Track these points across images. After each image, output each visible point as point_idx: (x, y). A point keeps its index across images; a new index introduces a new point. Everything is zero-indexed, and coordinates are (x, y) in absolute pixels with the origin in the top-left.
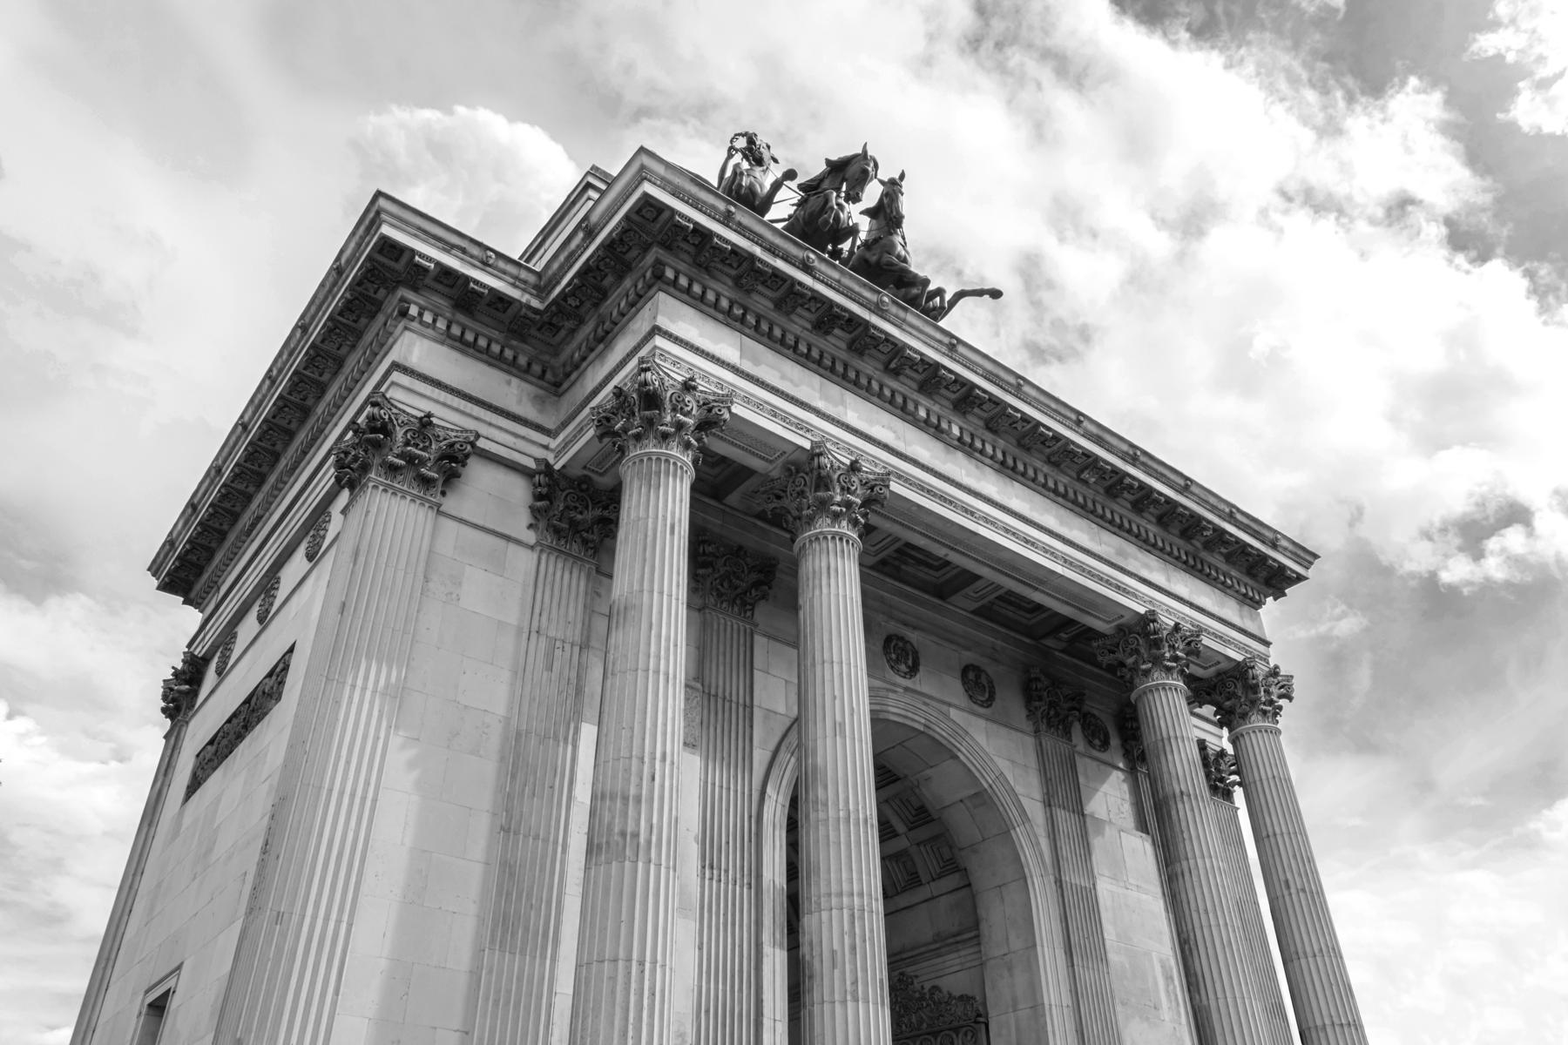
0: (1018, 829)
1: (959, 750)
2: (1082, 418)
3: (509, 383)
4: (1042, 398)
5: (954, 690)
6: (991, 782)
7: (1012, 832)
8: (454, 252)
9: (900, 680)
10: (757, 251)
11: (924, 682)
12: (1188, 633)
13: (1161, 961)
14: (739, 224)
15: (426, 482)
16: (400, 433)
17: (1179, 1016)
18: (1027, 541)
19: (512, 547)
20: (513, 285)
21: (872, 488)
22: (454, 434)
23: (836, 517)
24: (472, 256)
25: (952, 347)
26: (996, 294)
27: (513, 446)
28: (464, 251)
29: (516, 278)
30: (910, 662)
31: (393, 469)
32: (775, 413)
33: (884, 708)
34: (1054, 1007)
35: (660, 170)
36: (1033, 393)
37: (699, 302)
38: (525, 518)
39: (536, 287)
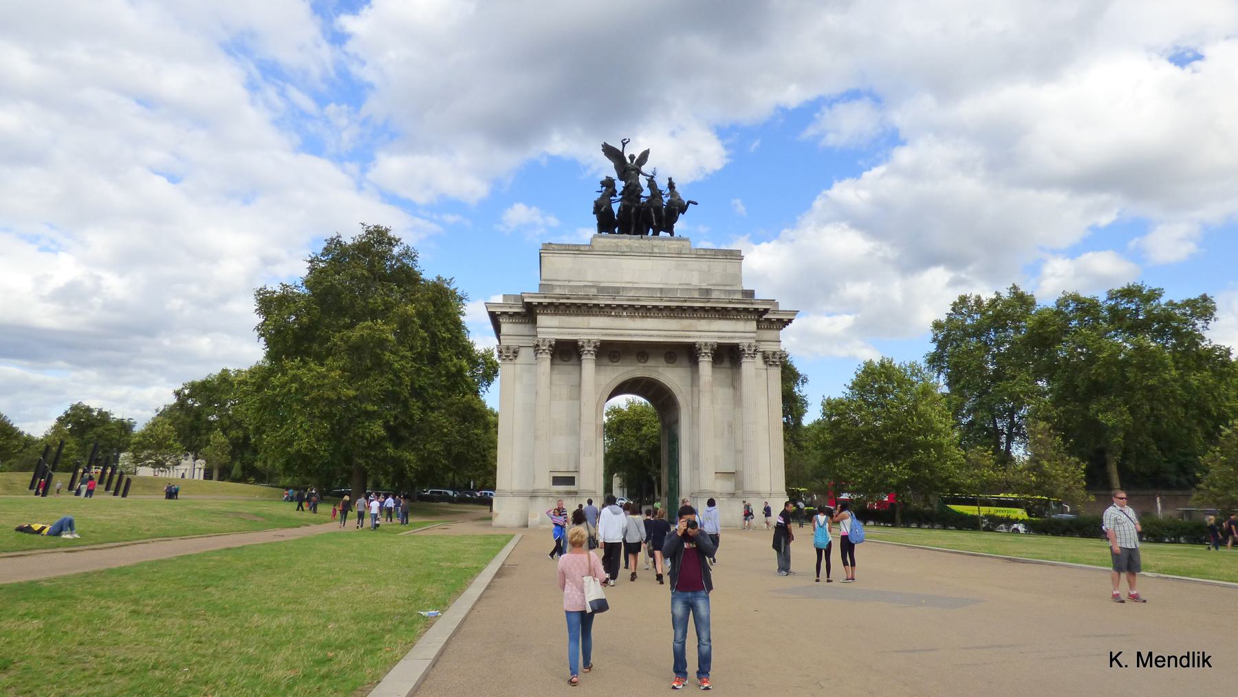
5: (662, 361)
9: (642, 365)
10: (554, 301)
11: (650, 363)
25: (614, 298)
32: (569, 334)
35: (527, 295)
37: (545, 314)
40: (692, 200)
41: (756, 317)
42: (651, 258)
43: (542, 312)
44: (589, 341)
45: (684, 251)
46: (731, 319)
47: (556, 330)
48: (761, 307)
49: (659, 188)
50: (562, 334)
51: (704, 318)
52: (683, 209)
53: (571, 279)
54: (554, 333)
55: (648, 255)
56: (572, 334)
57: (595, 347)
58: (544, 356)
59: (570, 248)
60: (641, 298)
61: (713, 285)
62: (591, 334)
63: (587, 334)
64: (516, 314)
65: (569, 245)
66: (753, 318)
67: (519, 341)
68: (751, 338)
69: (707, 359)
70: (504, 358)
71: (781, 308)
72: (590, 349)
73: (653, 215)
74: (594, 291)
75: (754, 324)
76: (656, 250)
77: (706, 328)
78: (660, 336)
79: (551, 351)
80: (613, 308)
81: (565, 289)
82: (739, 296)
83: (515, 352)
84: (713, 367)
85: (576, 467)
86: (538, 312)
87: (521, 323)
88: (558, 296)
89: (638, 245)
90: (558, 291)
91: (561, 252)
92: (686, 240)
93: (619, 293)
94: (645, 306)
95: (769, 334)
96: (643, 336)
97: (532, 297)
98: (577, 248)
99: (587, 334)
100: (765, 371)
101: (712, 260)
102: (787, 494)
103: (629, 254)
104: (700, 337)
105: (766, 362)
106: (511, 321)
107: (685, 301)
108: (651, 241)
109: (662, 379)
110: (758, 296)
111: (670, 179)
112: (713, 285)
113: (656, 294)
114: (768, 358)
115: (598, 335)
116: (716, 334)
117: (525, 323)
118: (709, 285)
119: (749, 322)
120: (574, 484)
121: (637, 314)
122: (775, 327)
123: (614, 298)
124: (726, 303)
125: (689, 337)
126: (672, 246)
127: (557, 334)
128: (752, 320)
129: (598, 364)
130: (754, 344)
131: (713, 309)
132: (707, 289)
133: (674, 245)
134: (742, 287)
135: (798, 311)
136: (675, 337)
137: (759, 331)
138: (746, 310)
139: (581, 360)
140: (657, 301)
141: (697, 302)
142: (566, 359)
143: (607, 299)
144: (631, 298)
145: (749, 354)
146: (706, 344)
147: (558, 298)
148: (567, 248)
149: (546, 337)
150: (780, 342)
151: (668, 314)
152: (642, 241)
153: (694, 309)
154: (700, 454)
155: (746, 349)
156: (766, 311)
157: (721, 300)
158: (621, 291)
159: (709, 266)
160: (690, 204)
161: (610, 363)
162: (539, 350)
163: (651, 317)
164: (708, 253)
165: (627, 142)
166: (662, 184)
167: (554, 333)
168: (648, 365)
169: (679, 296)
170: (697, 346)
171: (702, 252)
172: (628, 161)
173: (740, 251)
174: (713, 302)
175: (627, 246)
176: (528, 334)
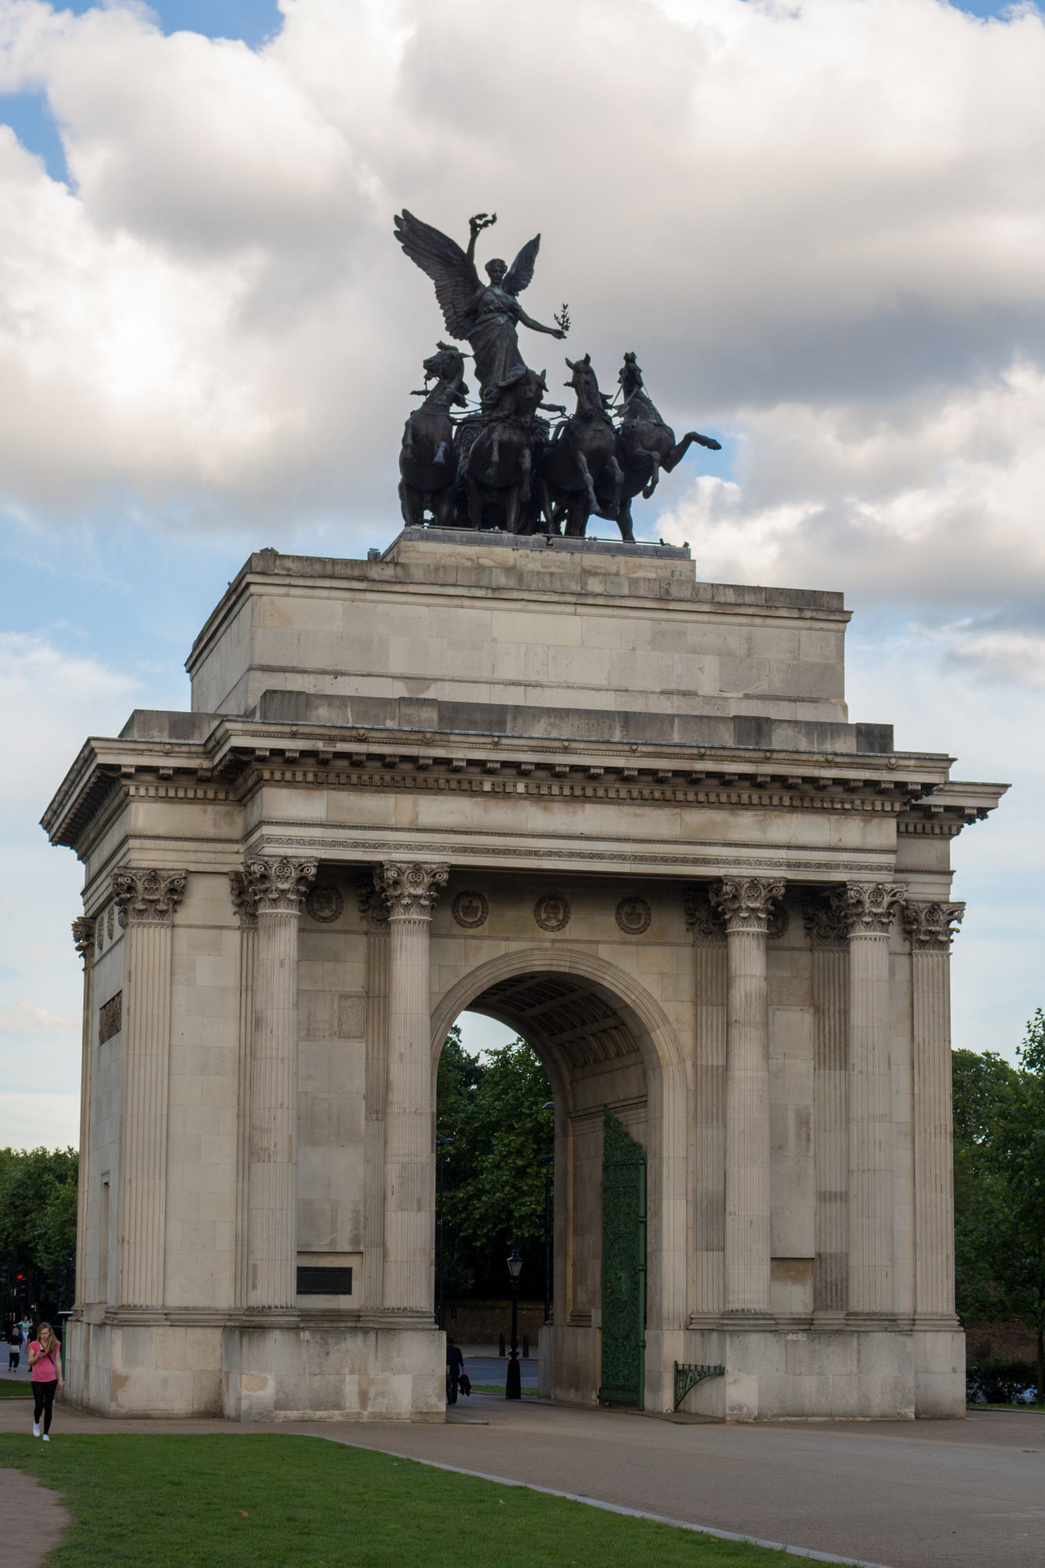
0: (658, 1031)
1: (604, 979)
2: (634, 747)
3: (205, 811)
4: (591, 746)
6: (634, 997)
7: (653, 1035)
8: (145, 753)
9: (551, 935)
10: (320, 745)
12: (772, 881)
13: (798, 1113)
14: (303, 734)
15: (162, 913)
16: (140, 886)
17: (807, 1149)
18: (592, 856)
19: (225, 932)
20: (189, 757)
21: (434, 876)
22: (172, 873)
23: (407, 906)
24: (157, 751)
26: (714, 445)
27: (214, 861)
28: (151, 751)
29: (190, 753)
30: (561, 917)
31: (141, 912)
32: (356, 845)
33: (529, 963)
34: (671, 1161)
36: (582, 745)
37: (292, 784)
38: (232, 909)
39: (204, 753)
40: (701, 432)
41: (897, 807)
42: (580, 609)
43: (278, 776)
44: (417, 867)
45: (675, 592)
46: (822, 811)
47: (317, 833)
48: (915, 778)
49: (603, 389)
50: (334, 844)
51: (749, 806)
52: (672, 455)
53: (341, 667)
54: (312, 842)
55: (573, 599)
56: (364, 846)
57: (434, 886)
58: (282, 910)
59: (339, 570)
60: (574, 745)
61: (763, 698)
62: (421, 847)
63: (408, 847)
64: (178, 771)
65: (334, 562)
66: (888, 808)
67: (192, 857)
68: (880, 868)
69: (755, 929)
70: (142, 907)
71: (955, 774)
72: (419, 891)
73: (588, 475)
74: (429, 717)
75: (892, 824)
76: (595, 585)
77: (755, 835)
78: (622, 857)
79: (303, 894)
80: (491, 772)
81: (346, 706)
82: (847, 745)
83: (172, 891)
84: (769, 949)
85: (356, 1240)
86: (267, 775)
87: (194, 801)
88: (335, 732)
89: (539, 568)
90: (323, 714)
91: (309, 582)
92: (683, 553)
93: (501, 724)
94: (584, 769)
95: (922, 851)
96: (572, 855)
97: (254, 734)
98: (356, 572)
99: (408, 847)
100: (905, 960)
101: (758, 621)
102: (962, 1323)
103: (515, 595)
104: (737, 862)
105: (908, 934)
106: (162, 792)
107: (701, 757)
108: (577, 556)
109: (607, 981)
110: (900, 745)
111: (630, 359)
112: (763, 698)
113: (611, 728)
114: (916, 920)
115: (441, 849)
116: (783, 854)
117: (204, 801)
118: (747, 697)
119: (875, 822)
120: (348, 1291)
121: (555, 790)
122: (937, 831)
123: (496, 744)
124: (817, 764)
125: (704, 861)
126: (640, 574)
127: (323, 843)
128: (884, 814)
129: (434, 933)
130: (889, 887)
131: (781, 780)
132: (757, 719)
133: (648, 569)
134: (845, 708)
135: (1006, 786)
136: (665, 860)
137: (906, 841)
138: (872, 785)
139: (388, 924)
140: (618, 753)
141: (733, 759)
142: (326, 913)
143: (474, 746)
144: (547, 743)
145: (876, 914)
146: (754, 883)
147: (332, 739)
148: (329, 570)
149: (289, 851)
150: (952, 873)
151: (646, 793)
152: (550, 554)
153: (724, 780)
154: (730, 1207)
155: (866, 899)
156: (928, 788)
157: (804, 757)
158: (509, 718)
159: (750, 639)
160: (694, 444)
161: (457, 929)
162: (266, 891)
163: (596, 800)
164: (749, 599)
165: (485, 225)
166: (610, 386)
167: (312, 842)
168: (568, 937)
169: (676, 738)
170: (727, 889)
171: (730, 597)
172: (485, 279)
173: (840, 596)
174: (778, 762)
175: (510, 570)
176: (210, 831)
